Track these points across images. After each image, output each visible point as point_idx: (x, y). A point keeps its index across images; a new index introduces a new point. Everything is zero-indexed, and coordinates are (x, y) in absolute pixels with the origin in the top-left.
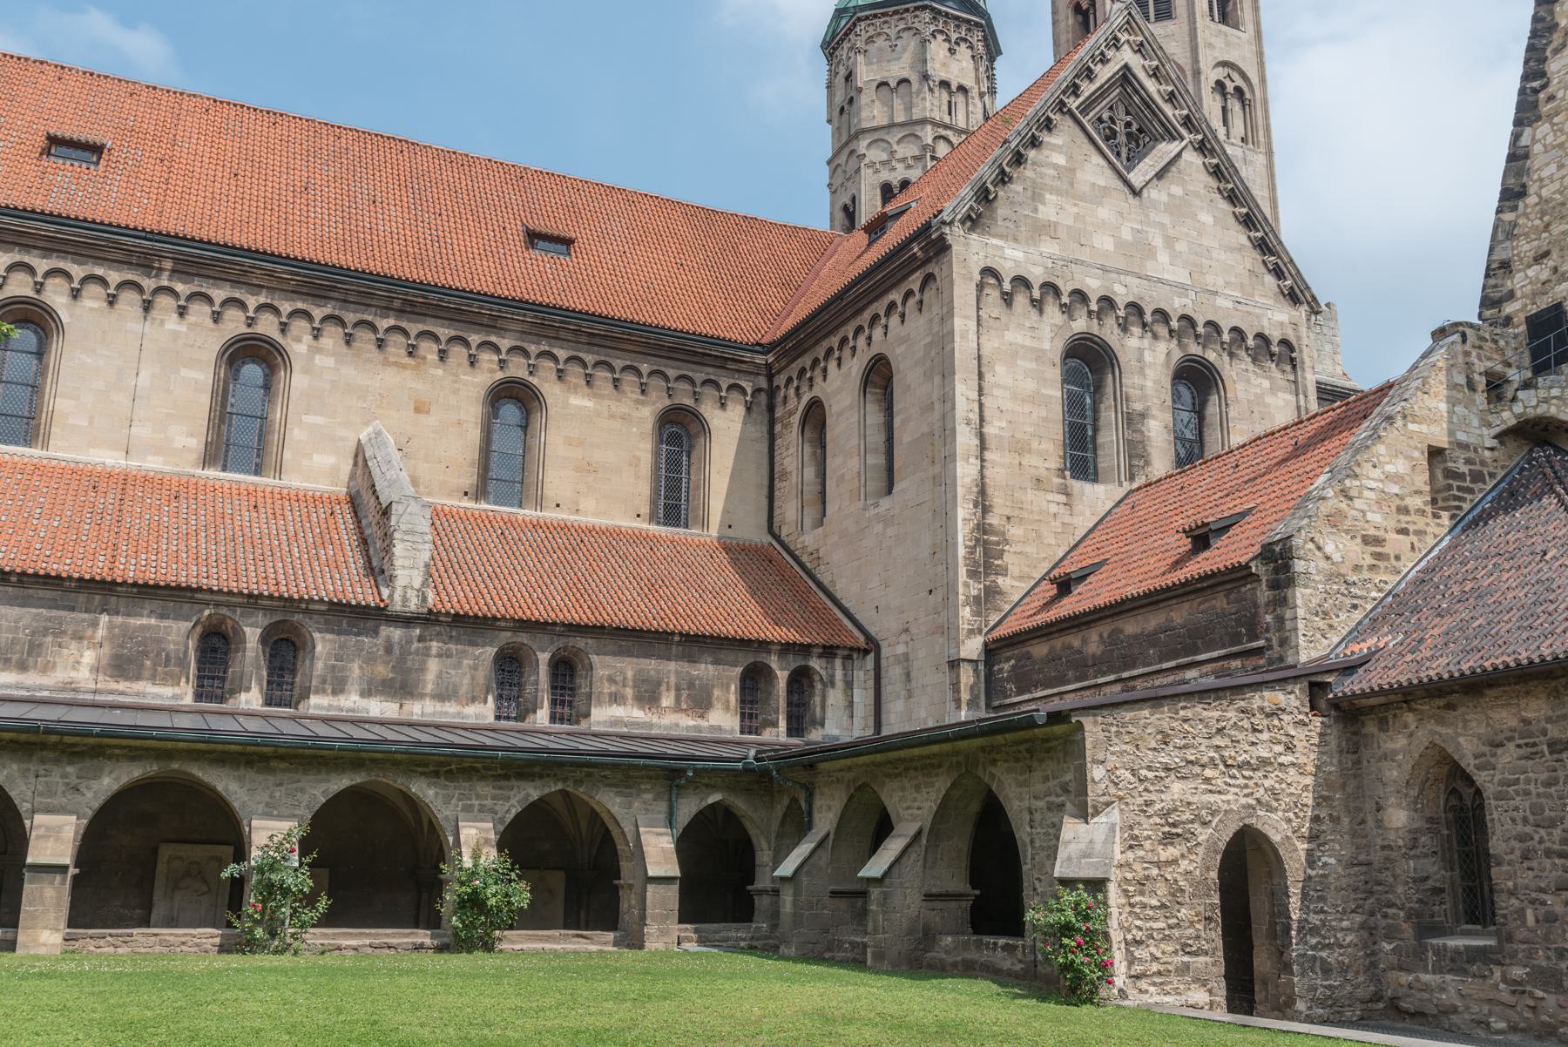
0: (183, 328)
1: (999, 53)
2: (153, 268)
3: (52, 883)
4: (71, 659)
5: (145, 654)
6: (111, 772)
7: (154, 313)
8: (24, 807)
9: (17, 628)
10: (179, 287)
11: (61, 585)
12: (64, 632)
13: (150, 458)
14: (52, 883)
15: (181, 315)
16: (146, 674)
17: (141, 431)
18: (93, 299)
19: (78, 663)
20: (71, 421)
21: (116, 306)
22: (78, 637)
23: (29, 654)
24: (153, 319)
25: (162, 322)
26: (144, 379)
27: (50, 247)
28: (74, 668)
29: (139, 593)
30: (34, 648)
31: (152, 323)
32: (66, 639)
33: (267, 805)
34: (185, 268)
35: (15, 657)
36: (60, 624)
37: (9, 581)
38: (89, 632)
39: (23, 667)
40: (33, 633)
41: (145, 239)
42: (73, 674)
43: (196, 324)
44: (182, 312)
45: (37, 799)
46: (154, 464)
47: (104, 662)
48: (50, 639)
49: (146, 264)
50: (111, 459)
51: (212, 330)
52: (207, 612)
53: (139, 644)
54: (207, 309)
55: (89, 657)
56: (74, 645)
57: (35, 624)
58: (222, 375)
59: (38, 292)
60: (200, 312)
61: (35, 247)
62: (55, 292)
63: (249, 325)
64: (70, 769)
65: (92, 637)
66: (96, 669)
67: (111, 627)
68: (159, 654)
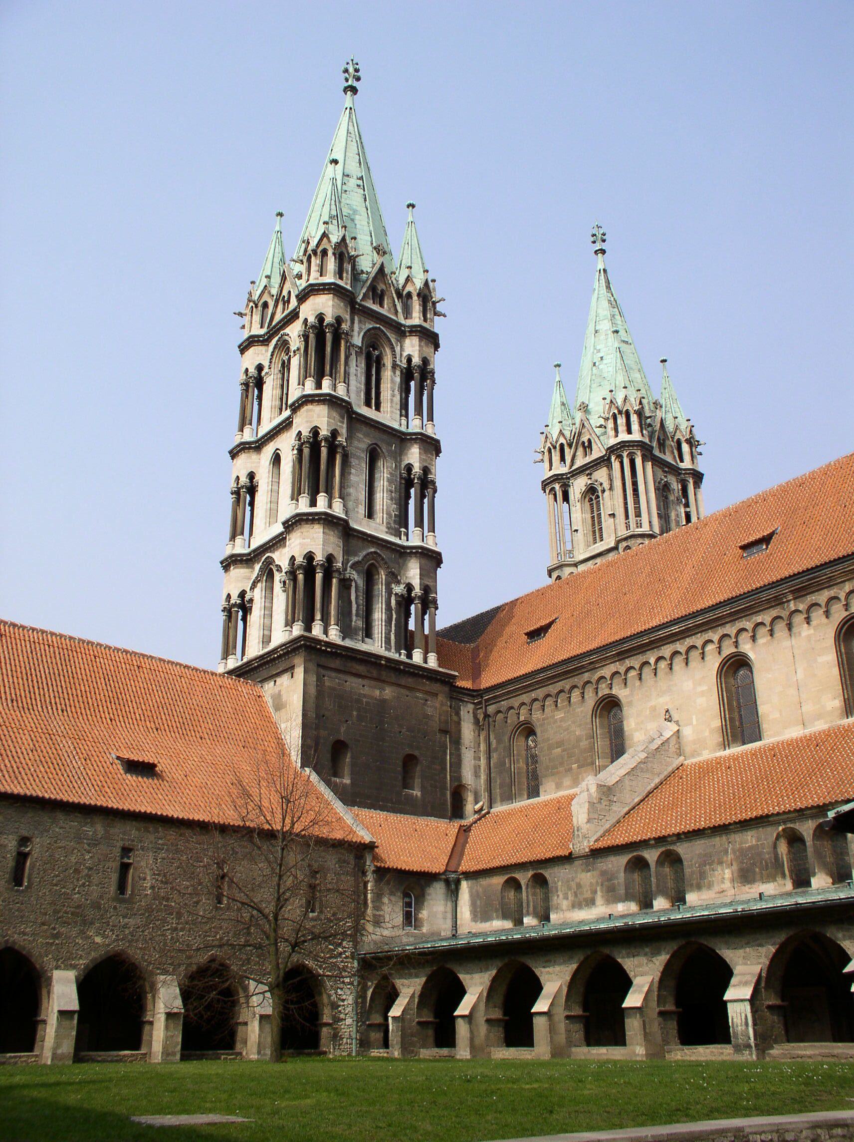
0: (812, 631)
1: (438, 442)
2: (784, 603)
3: (636, 1018)
4: (720, 877)
5: (754, 864)
6: (665, 949)
7: (794, 630)
8: (631, 975)
9: (692, 865)
10: (801, 607)
11: (704, 834)
12: (713, 862)
13: (816, 723)
14: (636, 1018)
15: (808, 623)
16: (758, 877)
17: (807, 708)
18: (763, 638)
19: (724, 878)
20: (771, 717)
21: (775, 636)
22: (720, 863)
23: (701, 879)
24: (795, 633)
25: (800, 633)
26: (800, 675)
27: (735, 616)
28: (723, 882)
29: (742, 827)
30: (702, 875)
31: (795, 637)
32: (715, 866)
33: (744, 957)
34: (800, 593)
35: (694, 882)
36: (711, 857)
37: (681, 839)
38: (725, 859)
39: (699, 887)
40: (699, 866)
41: (772, 588)
42: (723, 886)
43: (818, 625)
44: (808, 620)
45: (636, 969)
46: (820, 726)
47: (735, 875)
48: (708, 867)
49: (778, 601)
50: (795, 733)
51: (827, 624)
52: (780, 828)
53: (750, 859)
54: (821, 611)
55: (728, 873)
56: (719, 868)
57: (699, 860)
58: (843, 650)
59: (736, 647)
60: (818, 616)
61: (727, 623)
62: (744, 643)
63: (846, 610)
64: (647, 950)
65: (727, 861)
66: (732, 880)
67: (734, 852)
68: (761, 863)
